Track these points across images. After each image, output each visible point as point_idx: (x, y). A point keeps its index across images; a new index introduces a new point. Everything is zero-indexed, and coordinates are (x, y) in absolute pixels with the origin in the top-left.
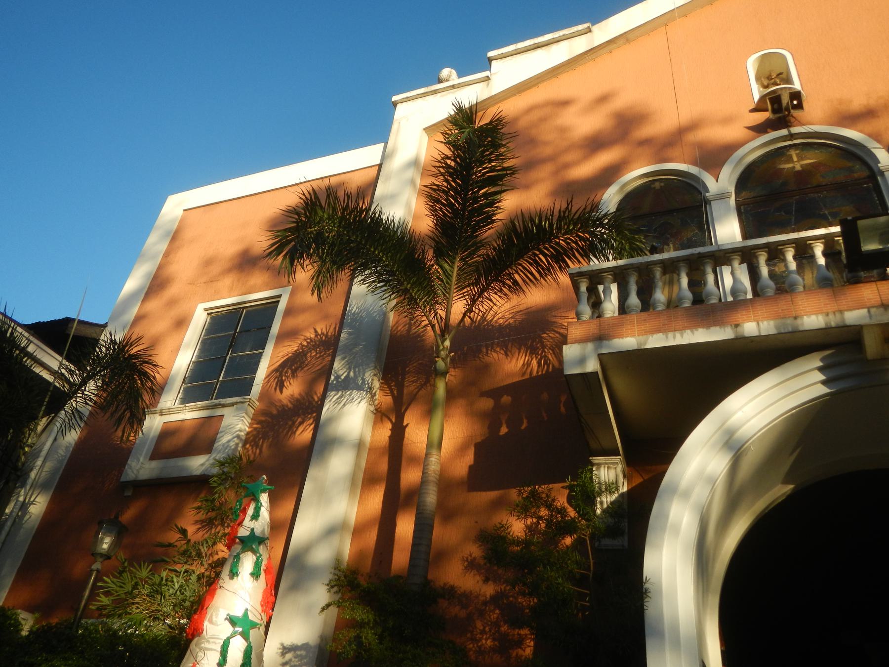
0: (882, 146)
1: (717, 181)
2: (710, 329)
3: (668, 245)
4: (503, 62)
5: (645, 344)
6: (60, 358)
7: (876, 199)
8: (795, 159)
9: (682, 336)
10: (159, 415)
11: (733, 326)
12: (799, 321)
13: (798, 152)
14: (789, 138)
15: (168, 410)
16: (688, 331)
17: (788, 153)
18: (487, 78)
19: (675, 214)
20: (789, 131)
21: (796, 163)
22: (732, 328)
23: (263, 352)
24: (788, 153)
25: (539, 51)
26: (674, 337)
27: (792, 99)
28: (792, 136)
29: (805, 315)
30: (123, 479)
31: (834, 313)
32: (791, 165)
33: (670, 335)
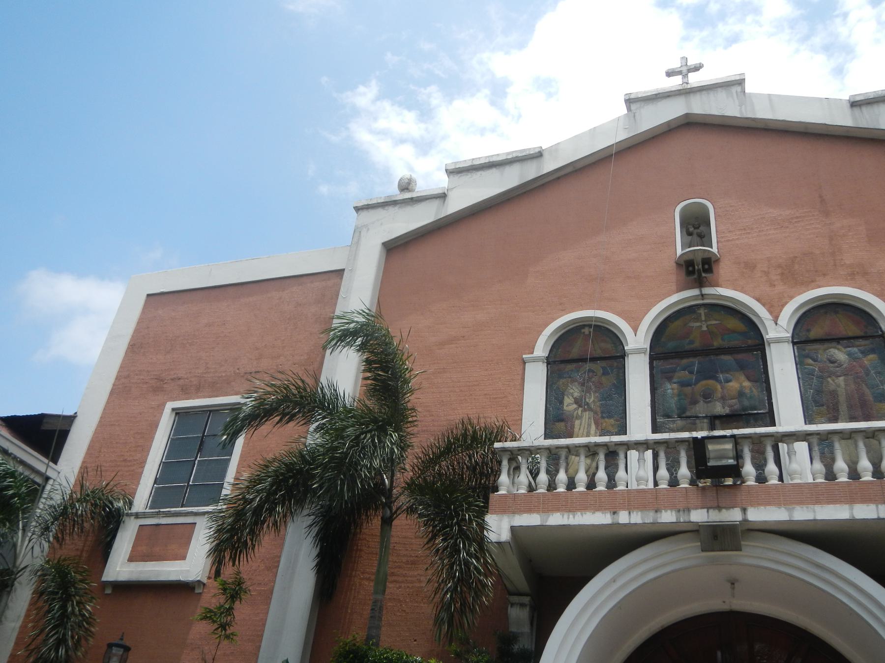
0: (773, 317)
1: (636, 336)
2: (594, 513)
3: (590, 394)
4: (461, 176)
5: (546, 522)
6: (46, 461)
7: (762, 367)
8: (703, 318)
9: (574, 517)
10: (135, 518)
11: (612, 512)
12: (659, 513)
13: (706, 311)
14: (700, 297)
15: (143, 514)
16: (579, 513)
17: (699, 312)
18: (443, 195)
19: (598, 362)
20: (701, 291)
21: (704, 323)
22: (611, 515)
23: (230, 460)
24: (699, 312)
25: (494, 170)
26: (568, 518)
27: (703, 264)
28: (703, 296)
29: (664, 509)
30: (104, 579)
31: (684, 510)
32: (698, 324)
33: (566, 516)
